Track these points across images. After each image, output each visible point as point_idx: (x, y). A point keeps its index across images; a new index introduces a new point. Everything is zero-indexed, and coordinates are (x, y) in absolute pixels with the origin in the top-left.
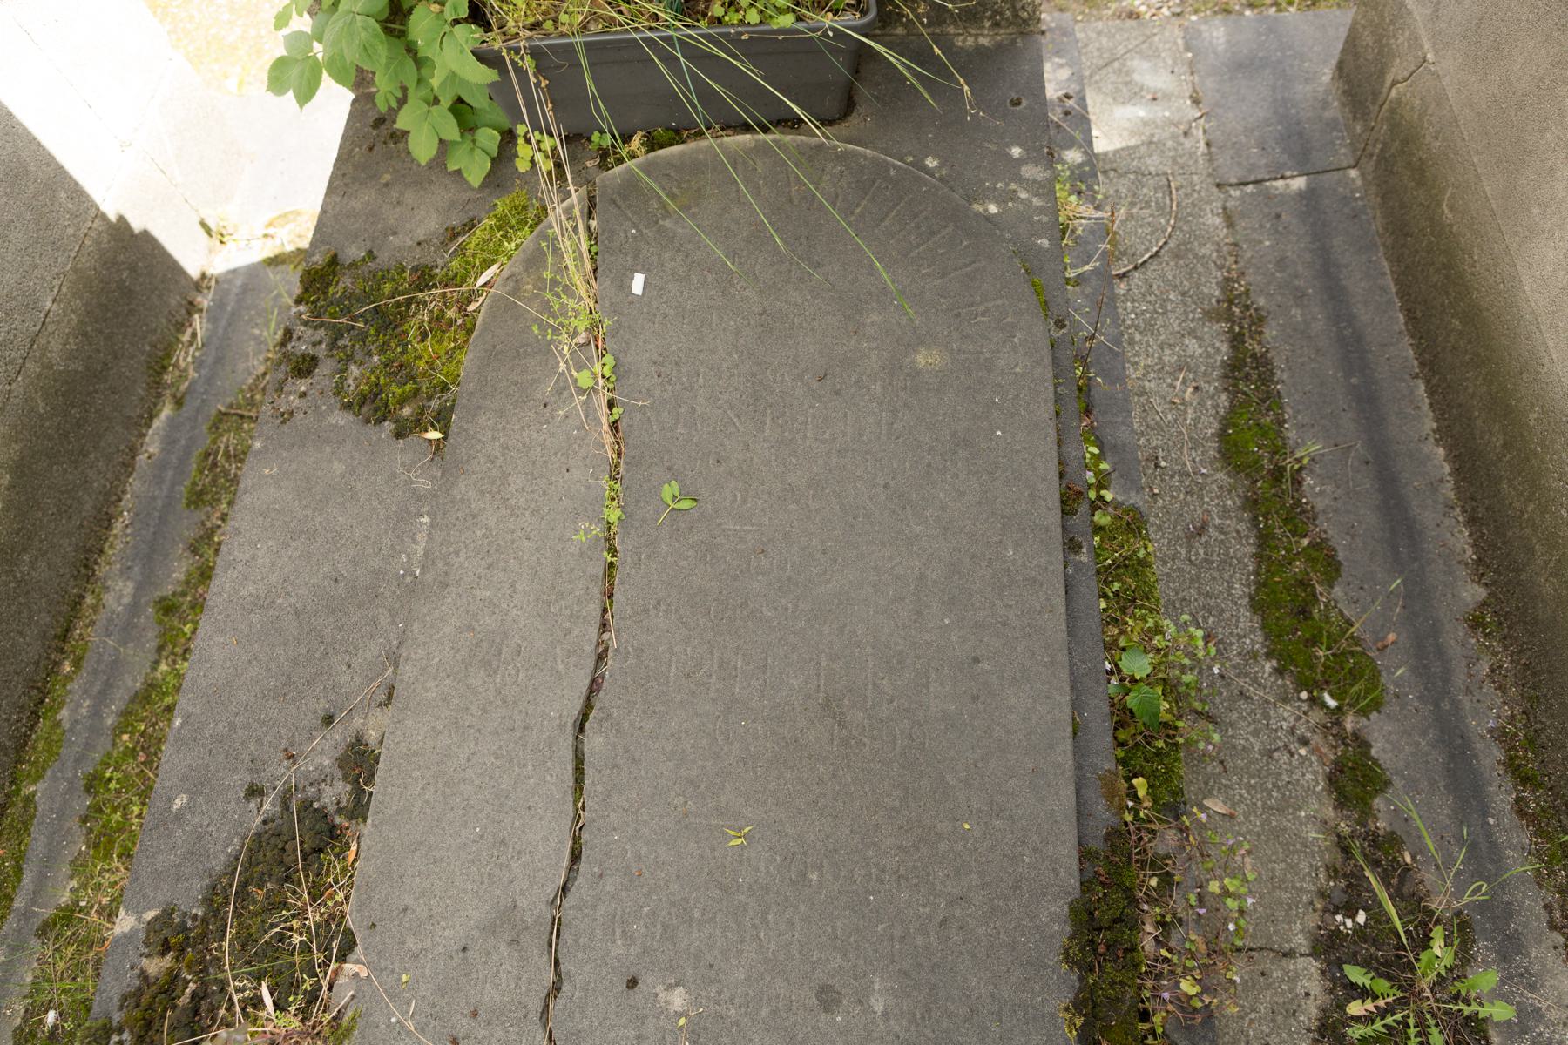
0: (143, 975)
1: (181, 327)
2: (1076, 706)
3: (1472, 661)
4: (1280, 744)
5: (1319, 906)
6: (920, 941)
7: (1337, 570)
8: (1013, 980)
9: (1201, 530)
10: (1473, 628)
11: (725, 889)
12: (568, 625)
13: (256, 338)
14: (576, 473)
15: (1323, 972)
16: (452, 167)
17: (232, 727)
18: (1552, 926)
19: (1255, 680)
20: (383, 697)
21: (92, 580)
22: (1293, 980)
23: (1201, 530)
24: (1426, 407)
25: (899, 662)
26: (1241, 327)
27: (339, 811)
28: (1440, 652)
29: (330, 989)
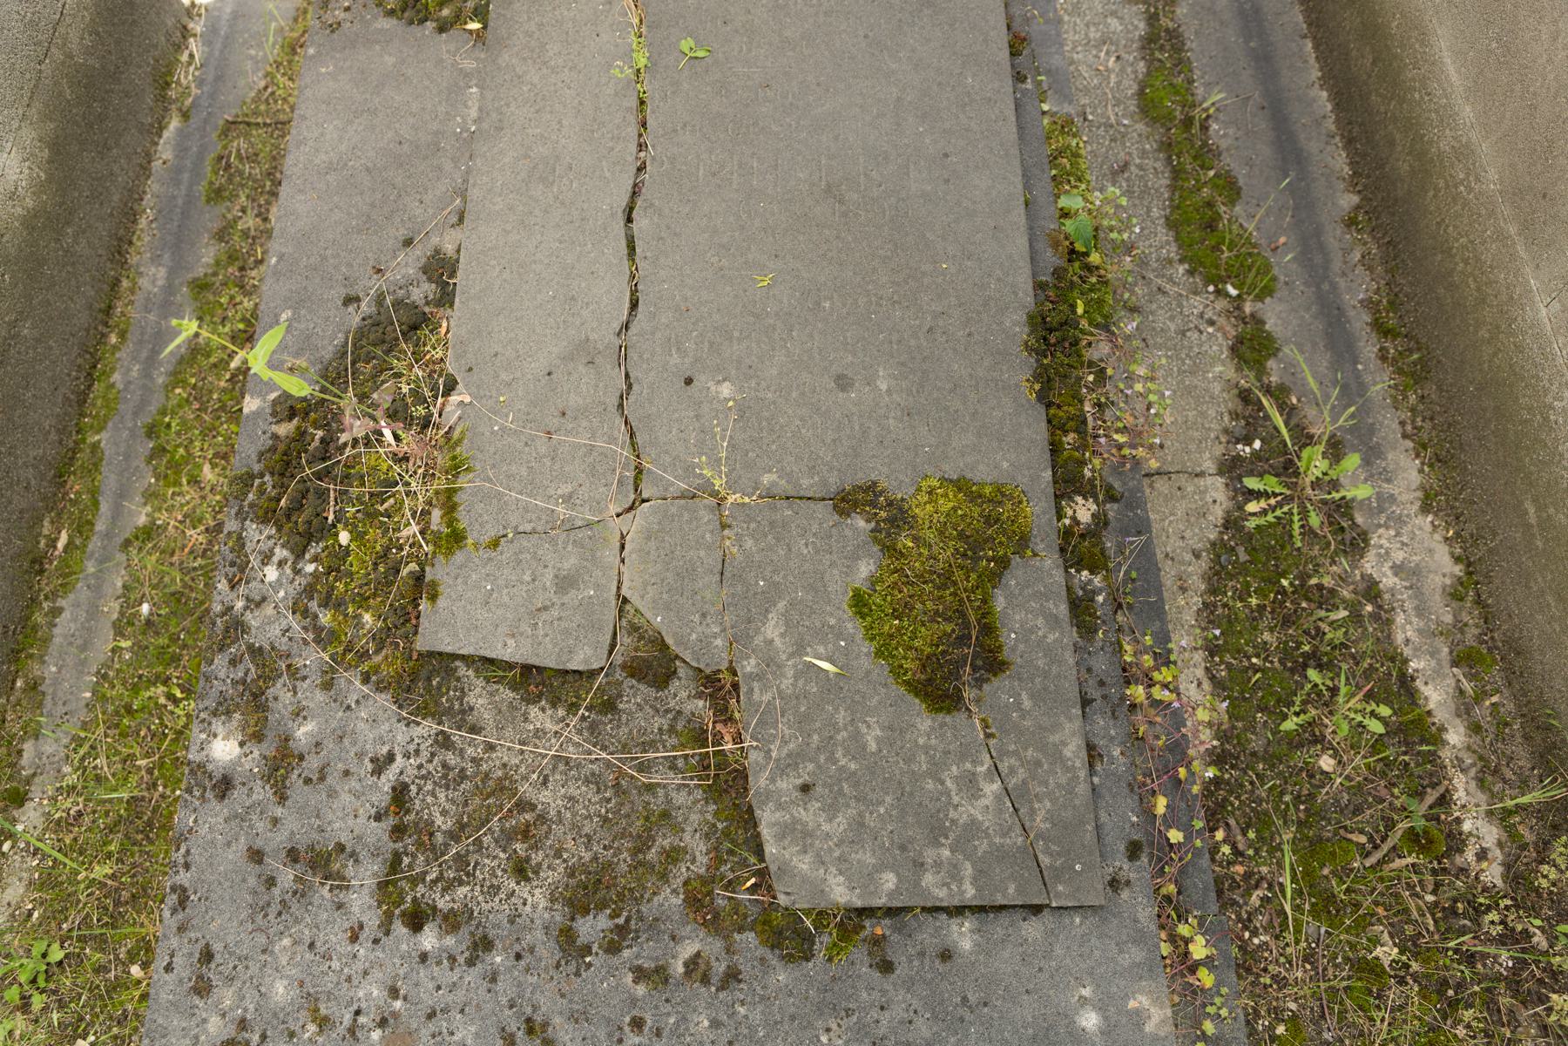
0: (275, 437)
1: (178, 48)
2: (1027, 186)
3: (1347, 252)
4: (1192, 325)
5: (1223, 440)
6: (913, 342)
7: (1238, 193)
8: (986, 364)
9: (1124, 167)
10: (1348, 226)
11: (757, 316)
12: (611, 144)
13: (252, 58)
14: (604, 37)
15: (1227, 485)
17: (324, 258)
18: (1405, 436)
19: (1171, 280)
20: (455, 219)
21: (126, 267)
22: (1203, 492)
23: (1124, 167)
24: (1312, 60)
25: (884, 159)
26: (1156, 9)
27: (427, 303)
28: (1322, 247)
29: (440, 416)
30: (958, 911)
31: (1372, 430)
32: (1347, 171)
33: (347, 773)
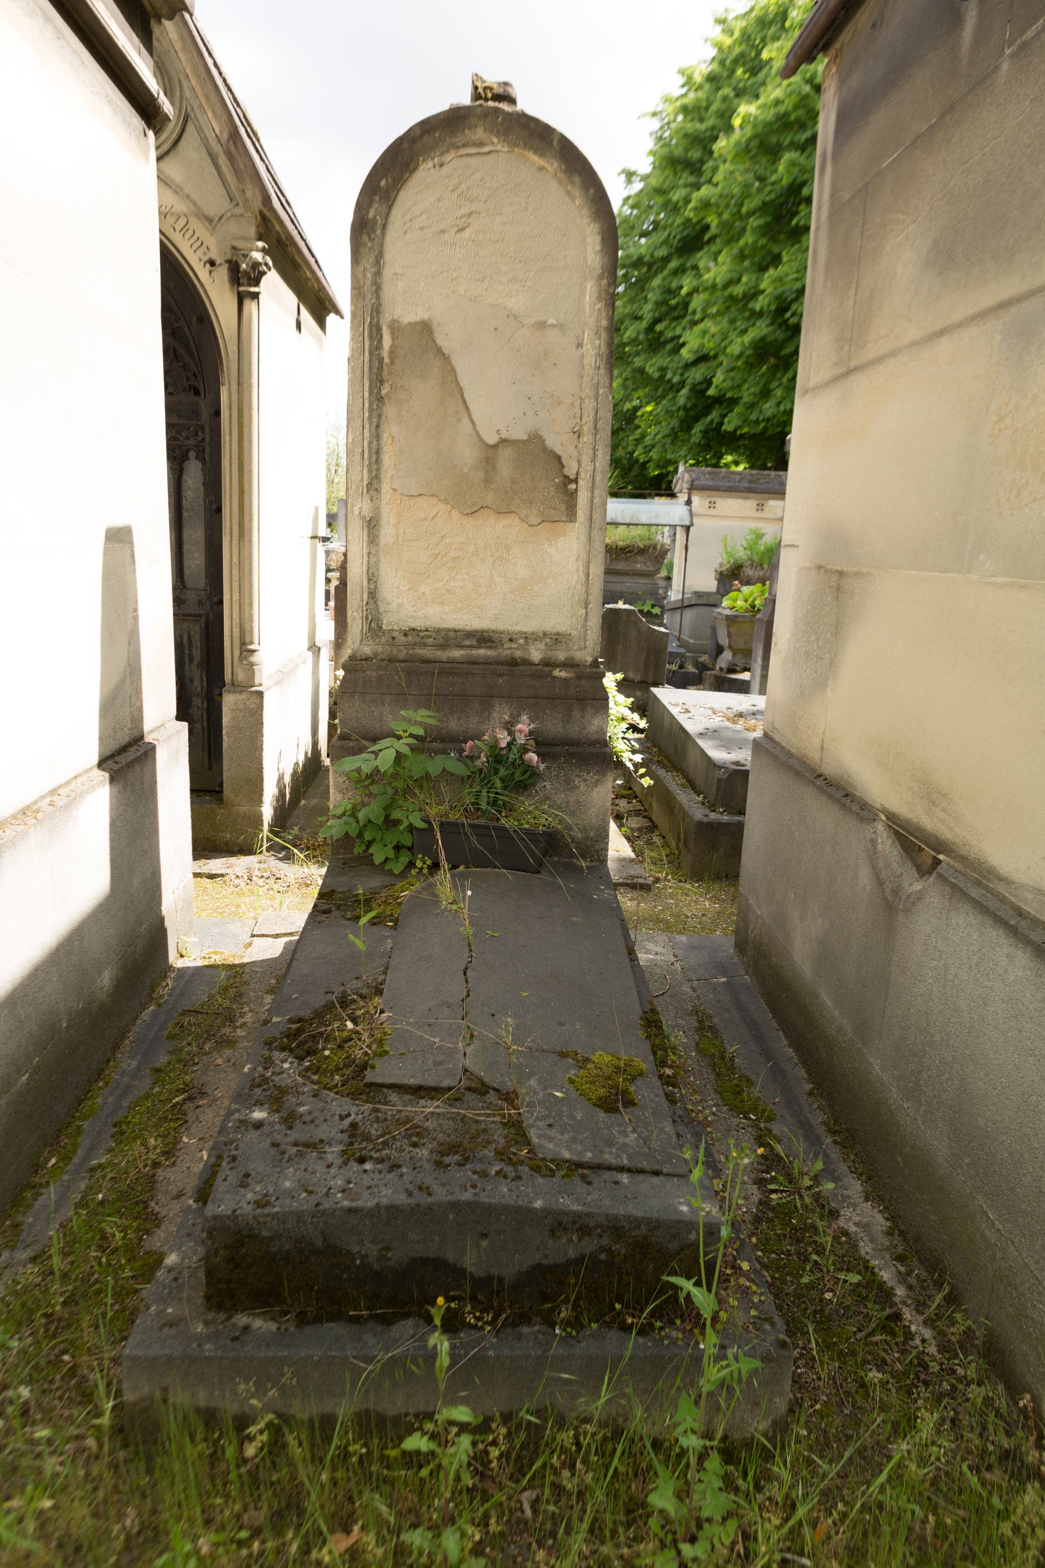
3: (810, 1105)
16: (387, 868)
18: (851, 1172)
30: (621, 1169)
31: (834, 1170)
32: (806, 1076)
33: (325, 1120)
